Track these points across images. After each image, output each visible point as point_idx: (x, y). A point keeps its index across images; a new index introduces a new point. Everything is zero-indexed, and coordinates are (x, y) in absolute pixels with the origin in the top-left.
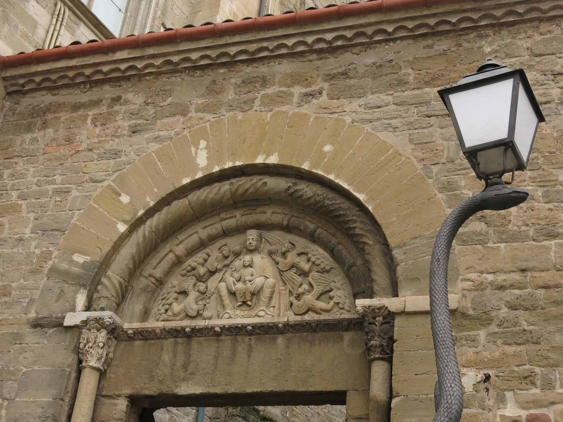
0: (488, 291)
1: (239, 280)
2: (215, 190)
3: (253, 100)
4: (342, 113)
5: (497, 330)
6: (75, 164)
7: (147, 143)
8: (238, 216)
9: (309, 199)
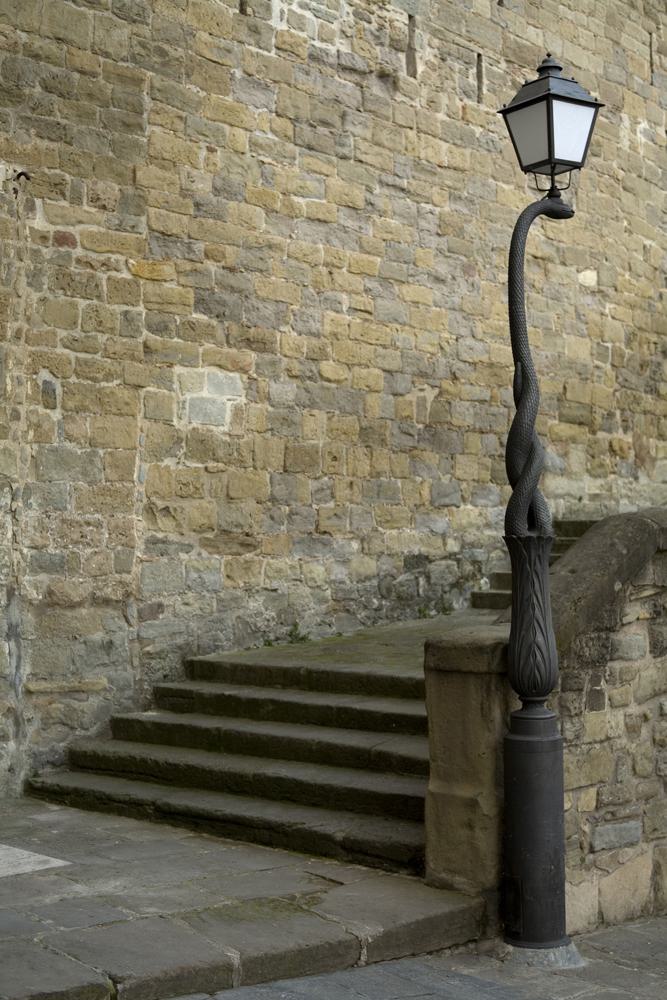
0: (20, 56)
5: (29, 114)
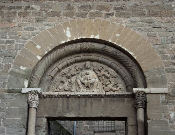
1: (85, 79)
2: (75, 47)
3: (86, 14)
4: (122, 23)
6: (14, 31)
7: (45, 26)
8: (82, 56)
9: (111, 52)
